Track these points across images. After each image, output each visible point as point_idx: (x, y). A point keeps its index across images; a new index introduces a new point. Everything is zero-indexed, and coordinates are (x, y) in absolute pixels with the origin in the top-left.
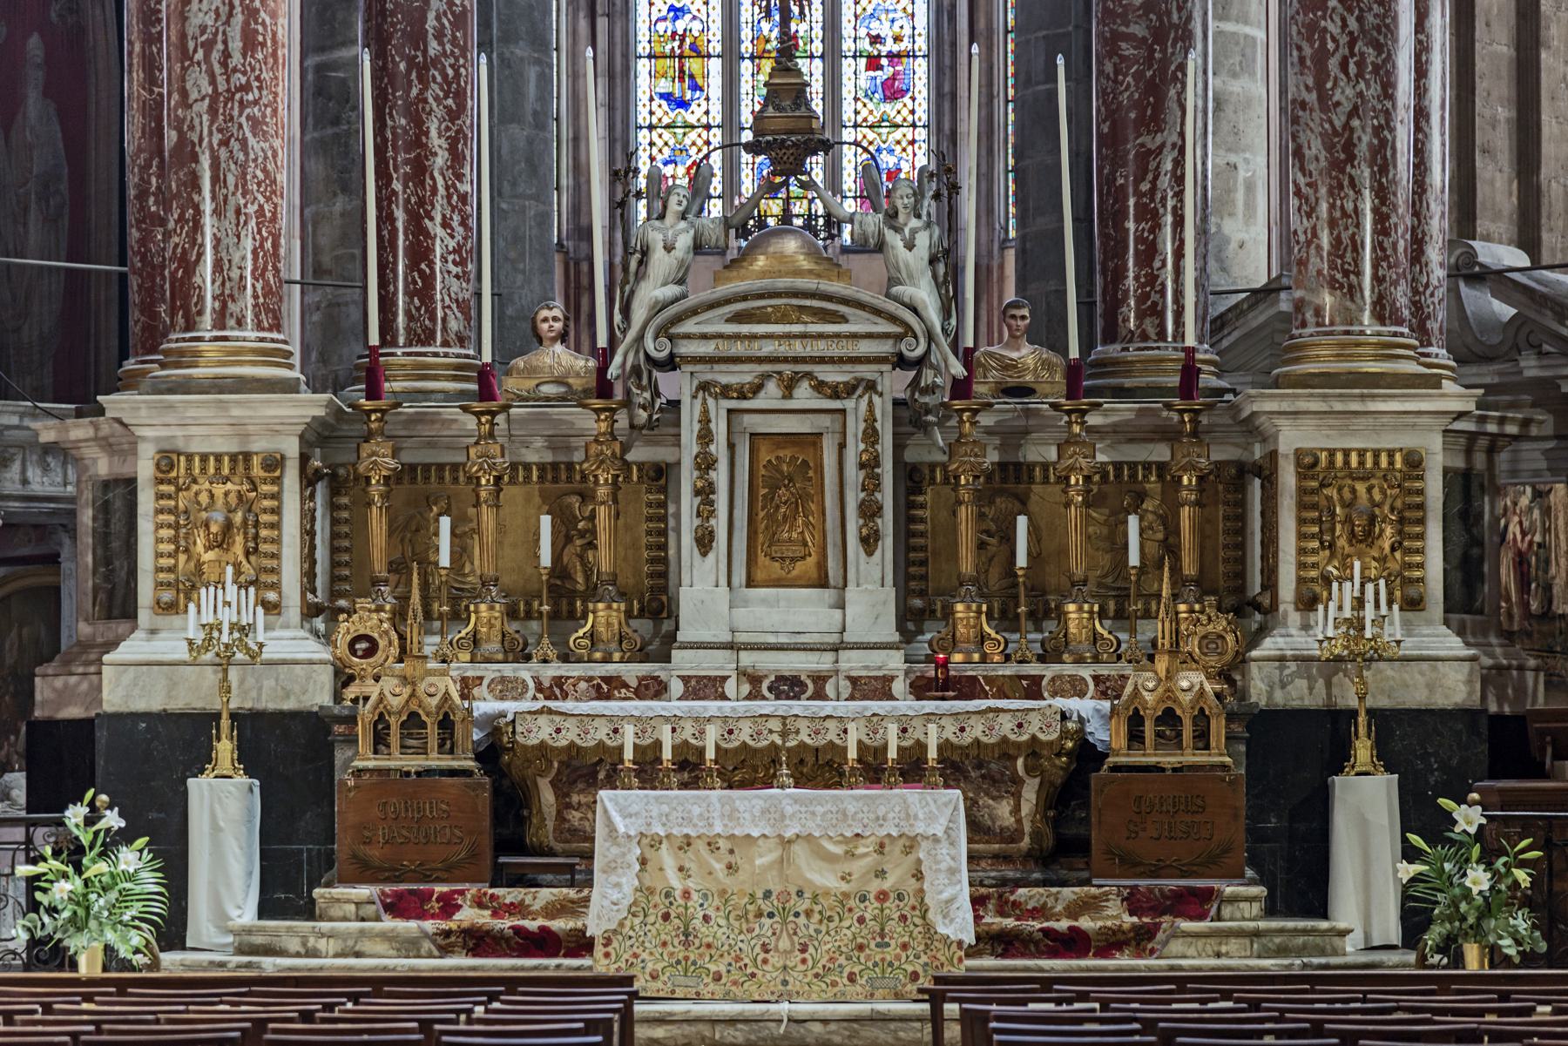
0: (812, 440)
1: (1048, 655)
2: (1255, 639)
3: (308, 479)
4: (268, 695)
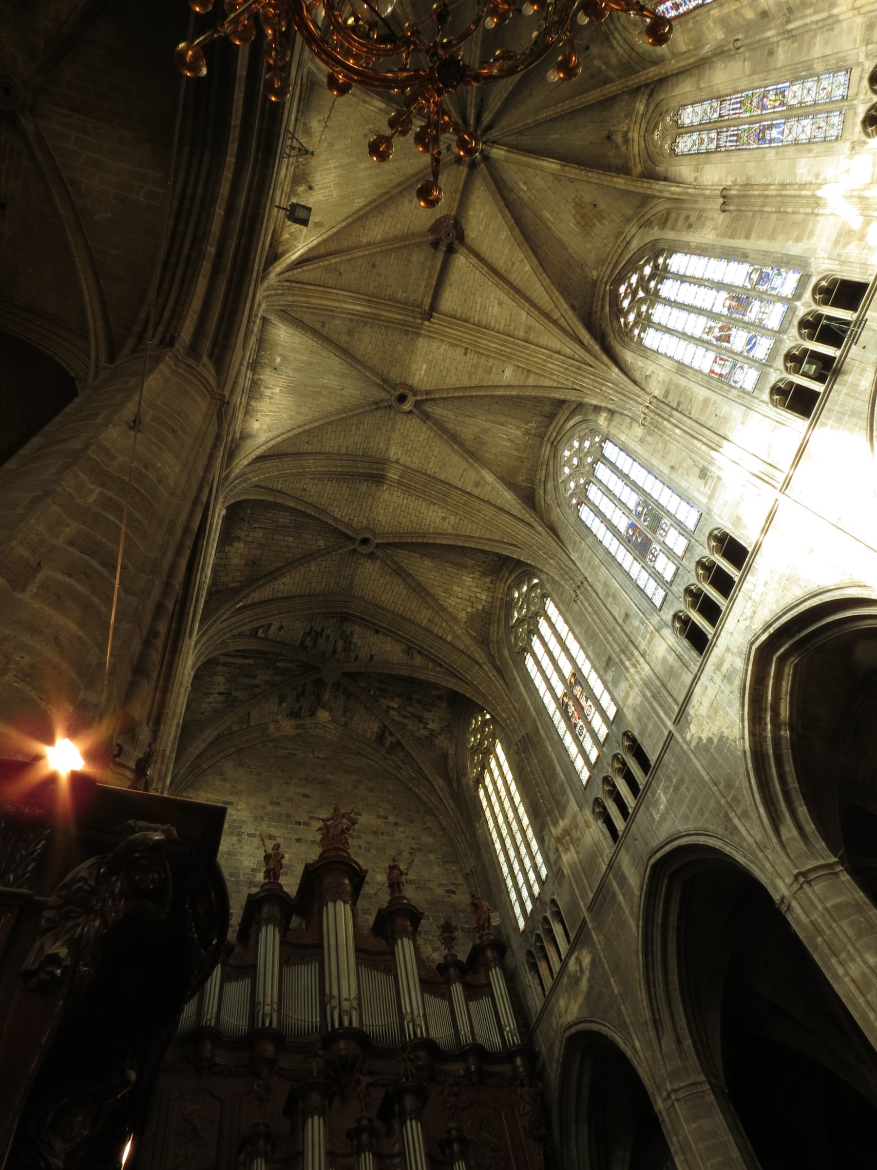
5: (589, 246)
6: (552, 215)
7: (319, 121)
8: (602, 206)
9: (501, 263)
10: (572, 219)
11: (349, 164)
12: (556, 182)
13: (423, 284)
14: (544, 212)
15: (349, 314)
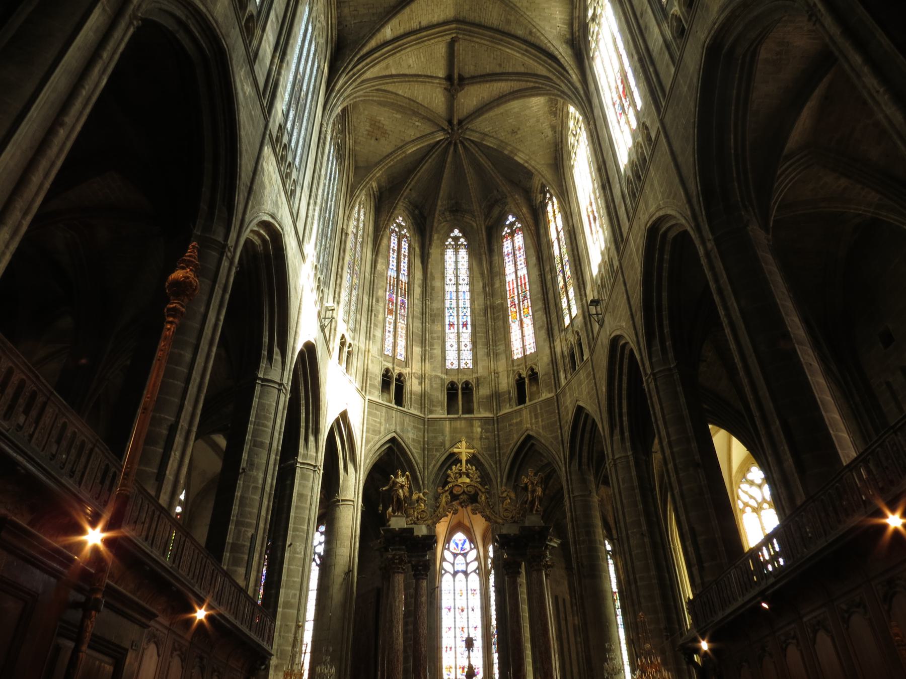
5: (366, 113)
6: (396, 117)
8: (373, 142)
9: (416, 86)
10: (384, 122)
12: (403, 138)
13: (461, 51)
14: (400, 117)
15: (513, 45)
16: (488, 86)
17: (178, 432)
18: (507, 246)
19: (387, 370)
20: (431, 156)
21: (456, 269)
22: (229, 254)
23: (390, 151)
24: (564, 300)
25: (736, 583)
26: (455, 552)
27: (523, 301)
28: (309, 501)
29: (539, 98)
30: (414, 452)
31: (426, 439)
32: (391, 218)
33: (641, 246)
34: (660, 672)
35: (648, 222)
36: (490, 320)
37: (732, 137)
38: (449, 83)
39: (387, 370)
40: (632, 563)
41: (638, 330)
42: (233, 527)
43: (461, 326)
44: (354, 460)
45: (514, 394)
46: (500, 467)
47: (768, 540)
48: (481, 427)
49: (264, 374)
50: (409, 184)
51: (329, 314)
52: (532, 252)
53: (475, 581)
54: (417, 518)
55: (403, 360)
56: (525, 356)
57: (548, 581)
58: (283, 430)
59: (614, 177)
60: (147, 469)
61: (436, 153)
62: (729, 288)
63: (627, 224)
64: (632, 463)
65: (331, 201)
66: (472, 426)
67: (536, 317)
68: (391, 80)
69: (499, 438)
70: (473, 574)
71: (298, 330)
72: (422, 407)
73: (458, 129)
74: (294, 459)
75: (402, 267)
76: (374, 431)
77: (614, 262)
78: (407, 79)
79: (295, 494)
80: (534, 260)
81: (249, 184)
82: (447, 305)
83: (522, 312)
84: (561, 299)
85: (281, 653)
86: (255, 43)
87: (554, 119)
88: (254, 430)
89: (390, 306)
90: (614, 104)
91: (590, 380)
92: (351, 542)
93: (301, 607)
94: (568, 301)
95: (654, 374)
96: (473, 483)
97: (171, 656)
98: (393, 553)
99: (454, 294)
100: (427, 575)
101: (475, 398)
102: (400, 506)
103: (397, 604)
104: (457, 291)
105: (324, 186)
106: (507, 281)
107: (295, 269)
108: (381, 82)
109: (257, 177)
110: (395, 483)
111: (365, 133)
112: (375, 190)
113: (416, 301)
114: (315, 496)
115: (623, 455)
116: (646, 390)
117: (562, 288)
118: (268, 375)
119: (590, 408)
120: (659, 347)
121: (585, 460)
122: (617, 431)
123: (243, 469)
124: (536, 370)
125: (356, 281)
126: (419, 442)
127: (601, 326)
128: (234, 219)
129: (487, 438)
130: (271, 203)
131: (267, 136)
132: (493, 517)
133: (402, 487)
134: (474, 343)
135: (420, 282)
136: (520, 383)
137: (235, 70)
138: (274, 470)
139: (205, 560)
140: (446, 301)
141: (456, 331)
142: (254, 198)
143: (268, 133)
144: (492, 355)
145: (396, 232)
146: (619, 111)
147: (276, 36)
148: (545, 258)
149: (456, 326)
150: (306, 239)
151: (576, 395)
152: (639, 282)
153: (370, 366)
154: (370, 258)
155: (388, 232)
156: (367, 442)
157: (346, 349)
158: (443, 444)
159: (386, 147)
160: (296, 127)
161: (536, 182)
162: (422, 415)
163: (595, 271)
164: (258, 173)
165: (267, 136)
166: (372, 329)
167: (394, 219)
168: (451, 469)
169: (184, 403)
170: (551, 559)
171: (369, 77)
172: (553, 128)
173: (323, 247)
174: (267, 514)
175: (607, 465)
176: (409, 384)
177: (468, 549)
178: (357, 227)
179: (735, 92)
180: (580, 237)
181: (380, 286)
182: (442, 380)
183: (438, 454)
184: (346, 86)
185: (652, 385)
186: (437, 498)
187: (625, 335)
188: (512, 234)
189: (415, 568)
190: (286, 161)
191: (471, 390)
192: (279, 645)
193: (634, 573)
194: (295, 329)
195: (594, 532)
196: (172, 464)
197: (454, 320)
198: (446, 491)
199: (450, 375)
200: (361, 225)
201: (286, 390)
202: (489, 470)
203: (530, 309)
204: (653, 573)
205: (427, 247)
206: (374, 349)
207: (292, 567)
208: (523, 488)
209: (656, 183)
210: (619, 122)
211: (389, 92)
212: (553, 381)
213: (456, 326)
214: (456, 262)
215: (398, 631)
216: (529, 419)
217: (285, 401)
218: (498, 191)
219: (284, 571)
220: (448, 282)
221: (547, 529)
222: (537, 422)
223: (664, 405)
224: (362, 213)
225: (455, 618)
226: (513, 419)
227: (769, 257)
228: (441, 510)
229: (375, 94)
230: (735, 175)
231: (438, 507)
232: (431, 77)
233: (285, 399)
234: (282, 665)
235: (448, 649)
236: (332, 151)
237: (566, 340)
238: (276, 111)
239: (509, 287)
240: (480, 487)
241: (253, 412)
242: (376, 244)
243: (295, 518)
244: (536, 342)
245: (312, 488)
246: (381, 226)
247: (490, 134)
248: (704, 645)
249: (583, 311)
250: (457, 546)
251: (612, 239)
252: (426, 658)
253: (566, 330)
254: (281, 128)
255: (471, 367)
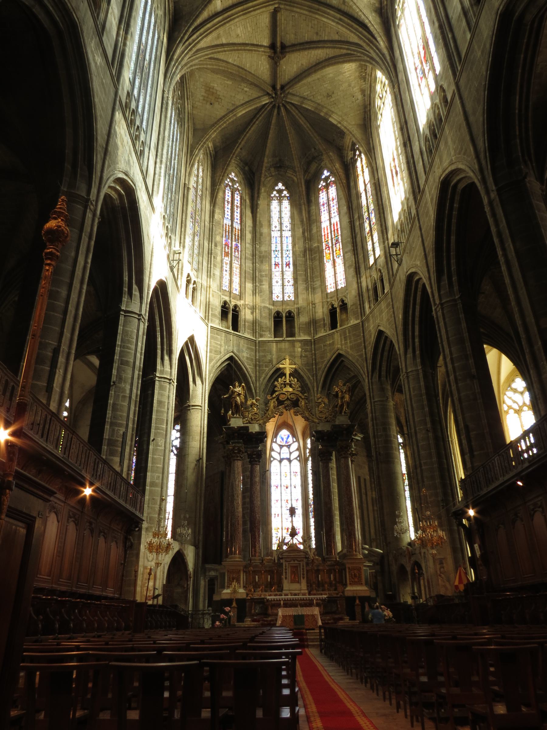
0: (296, 567)
1: (323, 590)
2: (345, 588)
3: (244, 572)
4: (239, 597)
5: (202, 80)
7: (358, 99)
8: (208, 106)
9: (244, 54)
10: (217, 89)
11: (339, 76)
15: (328, 14)
16: (306, 53)
17: (61, 354)
18: (323, 197)
19: (225, 303)
20: (258, 118)
21: (281, 217)
22: (92, 207)
23: (223, 114)
24: (370, 244)
25: (499, 467)
26: (281, 444)
27: (336, 244)
28: (166, 407)
29: (351, 64)
30: (248, 367)
31: (257, 358)
32: (225, 174)
33: (435, 197)
34: (437, 531)
35: (441, 175)
36: (308, 260)
37: (518, 98)
38: (272, 51)
39: (225, 303)
40: (419, 452)
41: (430, 268)
42: (108, 427)
43: (284, 266)
44: (200, 375)
45: (328, 321)
46: (317, 379)
47: (525, 434)
48: (301, 347)
49: (126, 307)
50: (240, 144)
51: (177, 257)
52: (344, 202)
53: (296, 466)
54: (251, 418)
55: (238, 294)
56: (337, 290)
57: (353, 465)
58: (143, 352)
59: (414, 135)
60: (38, 383)
61: (263, 116)
62: (507, 231)
63: (424, 177)
64: (421, 376)
65: (175, 159)
66: (294, 346)
67: (346, 257)
68: (223, 49)
69: (315, 356)
70: (295, 460)
71: (152, 270)
72: (254, 332)
73: (281, 94)
74: (153, 374)
75: (235, 216)
76: (216, 351)
77: (412, 210)
78: (236, 48)
79: (155, 401)
80: (345, 209)
81: (104, 146)
82: (273, 248)
83: (335, 253)
84: (367, 242)
85: (150, 520)
86: (102, 16)
87: (364, 83)
88: (121, 352)
89: (226, 249)
90: (416, 69)
91: (390, 309)
92: (200, 437)
93: (163, 486)
94: (373, 244)
95: (442, 304)
96: (295, 392)
97: (68, 522)
98: (234, 445)
99: (279, 239)
100: (259, 462)
101: (296, 324)
102: (238, 410)
103: (237, 483)
104: (281, 237)
105: (168, 146)
106: (323, 228)
107: (147, 219)
108: (213, 51)
109: (111, 140)
110: (233, 392)
111: (202, 98)
112: (211, 149)
113: (247, 245)
114: (171, 402)
115: (414, 369)
116: (435, 317)
117: (368, 233)
118: (129, 307)
119: (389, 332)
120: (447, 282)
121: (383, 373)
122: (410, 350)
123: (114, 382)
124: (346, 302)
125: (197, 228)
126: (252, 360)
127: (400, 265)
128: (94, 177)
129: (306, 356)
130: (124, 162)
131: (118, 102)
132: (310, 418)
133: (239, 395)
134: (295, 279)
135: (251, 229)
136: (333, 313)
137: (86, 41)
138: (138, 383)
139: (88, 451)
140: (272, 245)
141: (281, 270)
142: (110, 158)
143: (118, 99)
144: (310, 290)
145: (230, 186)
146: (420, 75)
147: (120, 9)
148: (354, 207)
149: (280, 266)
150: (155, 193)
151: (378, 321)
152: (432, 228)
153: (211, 300)
154: (209, 209)
155: (223, 186)
156: (211, 360)
157: (191, 286)
158: (271, 361)
159: (219, 111)
160: (142, 94)
161: (348, 141)
162: (254, 339)
163: (396, 218)
164: (112, 136)
165: (118, 102)
166: (212, 269)
167: (228, 175)
168: (278, 381)
169: (63, 331)
170: (355, 449)
171: (203, 46)
172: (363, 91)
173: (169, 200)
174: (134, 416)
175: (401, 377)
176: (243, 314)
177: (292, 442)
178: (197, 182)
179: (522, 56)
180: (384, 189)
181: (217, 232)
182: (270, 310)
183: (267, 369)
184: (183, 55)
185: (440, 313)
186: (267, 403)
187: (420, 272)
188: (327, 187)
189: (250, 456)
190: (135, 125)
191: (293, 317)
192: (148, 514)
193: (420, 460)
194: (149, 269)
195: (389, 429)
196: (58, 379)
197: (279, 260)
198: (274, 398)
199: (276, 306)
200: (200, 180)
201: (144, 319)
202: (308, 382)
203: (341, 250)
204: (434, 459)
205: (256, 199)
206: (214, 286)
207: (155, 456)
208: (334, 395)
209: (449, 140)
210: (419, 85)
211: (220, 60)
212: (359, 310)
213: (280, 266)
214: (280, 212)
215: (238, 503)
216: (339, 341)
217: (144, 328)
218: (315, 149)
219: (150, 459)
220: (274, 228)
221: (353, 426)
222: (346, 344)
223: (448, 329)
224: (201, 170)
225: (281, 493)
226: (327, 341)
227: (542, 205)
228: (270, 413)
229: (208, 63)
230: (517, 133)
231: (267, 410)
232: (257, 45)
233: (143, 327)
234: (151, 528)
235: (276, 515)
236: (173, 115)
237: (371, 276)
238: (124, 80)
239: (324, 232)
240: (300, 395)
241: (119, 338)
242: (213, 197)
243: (156, 419)
244: (346, 278)
245: (169, 397)
246: (217, 181)
247: (309, 98)
248: (471, 513)
249: (385, 252)
250: (283, 440)
251: (411, 190)
252: (259, 522)
253: (370, 268)
254: (129, 95)
255: (293, 299)
